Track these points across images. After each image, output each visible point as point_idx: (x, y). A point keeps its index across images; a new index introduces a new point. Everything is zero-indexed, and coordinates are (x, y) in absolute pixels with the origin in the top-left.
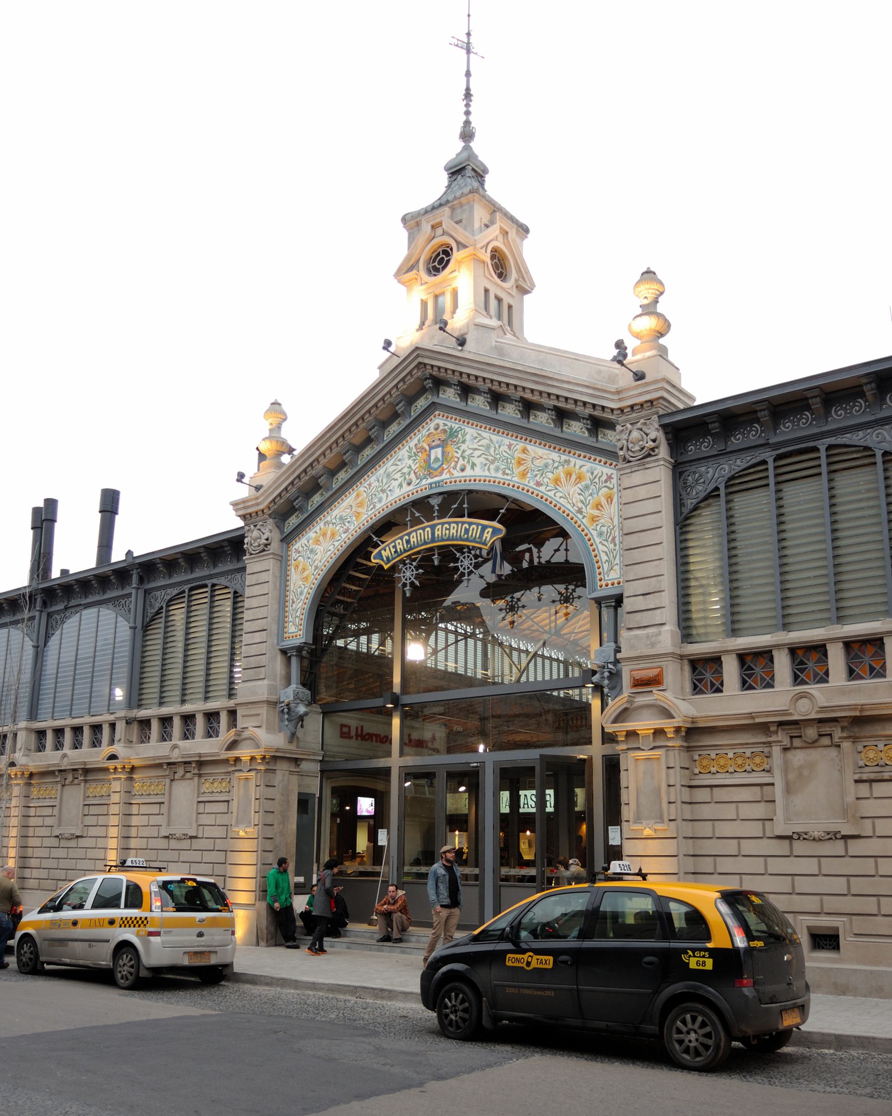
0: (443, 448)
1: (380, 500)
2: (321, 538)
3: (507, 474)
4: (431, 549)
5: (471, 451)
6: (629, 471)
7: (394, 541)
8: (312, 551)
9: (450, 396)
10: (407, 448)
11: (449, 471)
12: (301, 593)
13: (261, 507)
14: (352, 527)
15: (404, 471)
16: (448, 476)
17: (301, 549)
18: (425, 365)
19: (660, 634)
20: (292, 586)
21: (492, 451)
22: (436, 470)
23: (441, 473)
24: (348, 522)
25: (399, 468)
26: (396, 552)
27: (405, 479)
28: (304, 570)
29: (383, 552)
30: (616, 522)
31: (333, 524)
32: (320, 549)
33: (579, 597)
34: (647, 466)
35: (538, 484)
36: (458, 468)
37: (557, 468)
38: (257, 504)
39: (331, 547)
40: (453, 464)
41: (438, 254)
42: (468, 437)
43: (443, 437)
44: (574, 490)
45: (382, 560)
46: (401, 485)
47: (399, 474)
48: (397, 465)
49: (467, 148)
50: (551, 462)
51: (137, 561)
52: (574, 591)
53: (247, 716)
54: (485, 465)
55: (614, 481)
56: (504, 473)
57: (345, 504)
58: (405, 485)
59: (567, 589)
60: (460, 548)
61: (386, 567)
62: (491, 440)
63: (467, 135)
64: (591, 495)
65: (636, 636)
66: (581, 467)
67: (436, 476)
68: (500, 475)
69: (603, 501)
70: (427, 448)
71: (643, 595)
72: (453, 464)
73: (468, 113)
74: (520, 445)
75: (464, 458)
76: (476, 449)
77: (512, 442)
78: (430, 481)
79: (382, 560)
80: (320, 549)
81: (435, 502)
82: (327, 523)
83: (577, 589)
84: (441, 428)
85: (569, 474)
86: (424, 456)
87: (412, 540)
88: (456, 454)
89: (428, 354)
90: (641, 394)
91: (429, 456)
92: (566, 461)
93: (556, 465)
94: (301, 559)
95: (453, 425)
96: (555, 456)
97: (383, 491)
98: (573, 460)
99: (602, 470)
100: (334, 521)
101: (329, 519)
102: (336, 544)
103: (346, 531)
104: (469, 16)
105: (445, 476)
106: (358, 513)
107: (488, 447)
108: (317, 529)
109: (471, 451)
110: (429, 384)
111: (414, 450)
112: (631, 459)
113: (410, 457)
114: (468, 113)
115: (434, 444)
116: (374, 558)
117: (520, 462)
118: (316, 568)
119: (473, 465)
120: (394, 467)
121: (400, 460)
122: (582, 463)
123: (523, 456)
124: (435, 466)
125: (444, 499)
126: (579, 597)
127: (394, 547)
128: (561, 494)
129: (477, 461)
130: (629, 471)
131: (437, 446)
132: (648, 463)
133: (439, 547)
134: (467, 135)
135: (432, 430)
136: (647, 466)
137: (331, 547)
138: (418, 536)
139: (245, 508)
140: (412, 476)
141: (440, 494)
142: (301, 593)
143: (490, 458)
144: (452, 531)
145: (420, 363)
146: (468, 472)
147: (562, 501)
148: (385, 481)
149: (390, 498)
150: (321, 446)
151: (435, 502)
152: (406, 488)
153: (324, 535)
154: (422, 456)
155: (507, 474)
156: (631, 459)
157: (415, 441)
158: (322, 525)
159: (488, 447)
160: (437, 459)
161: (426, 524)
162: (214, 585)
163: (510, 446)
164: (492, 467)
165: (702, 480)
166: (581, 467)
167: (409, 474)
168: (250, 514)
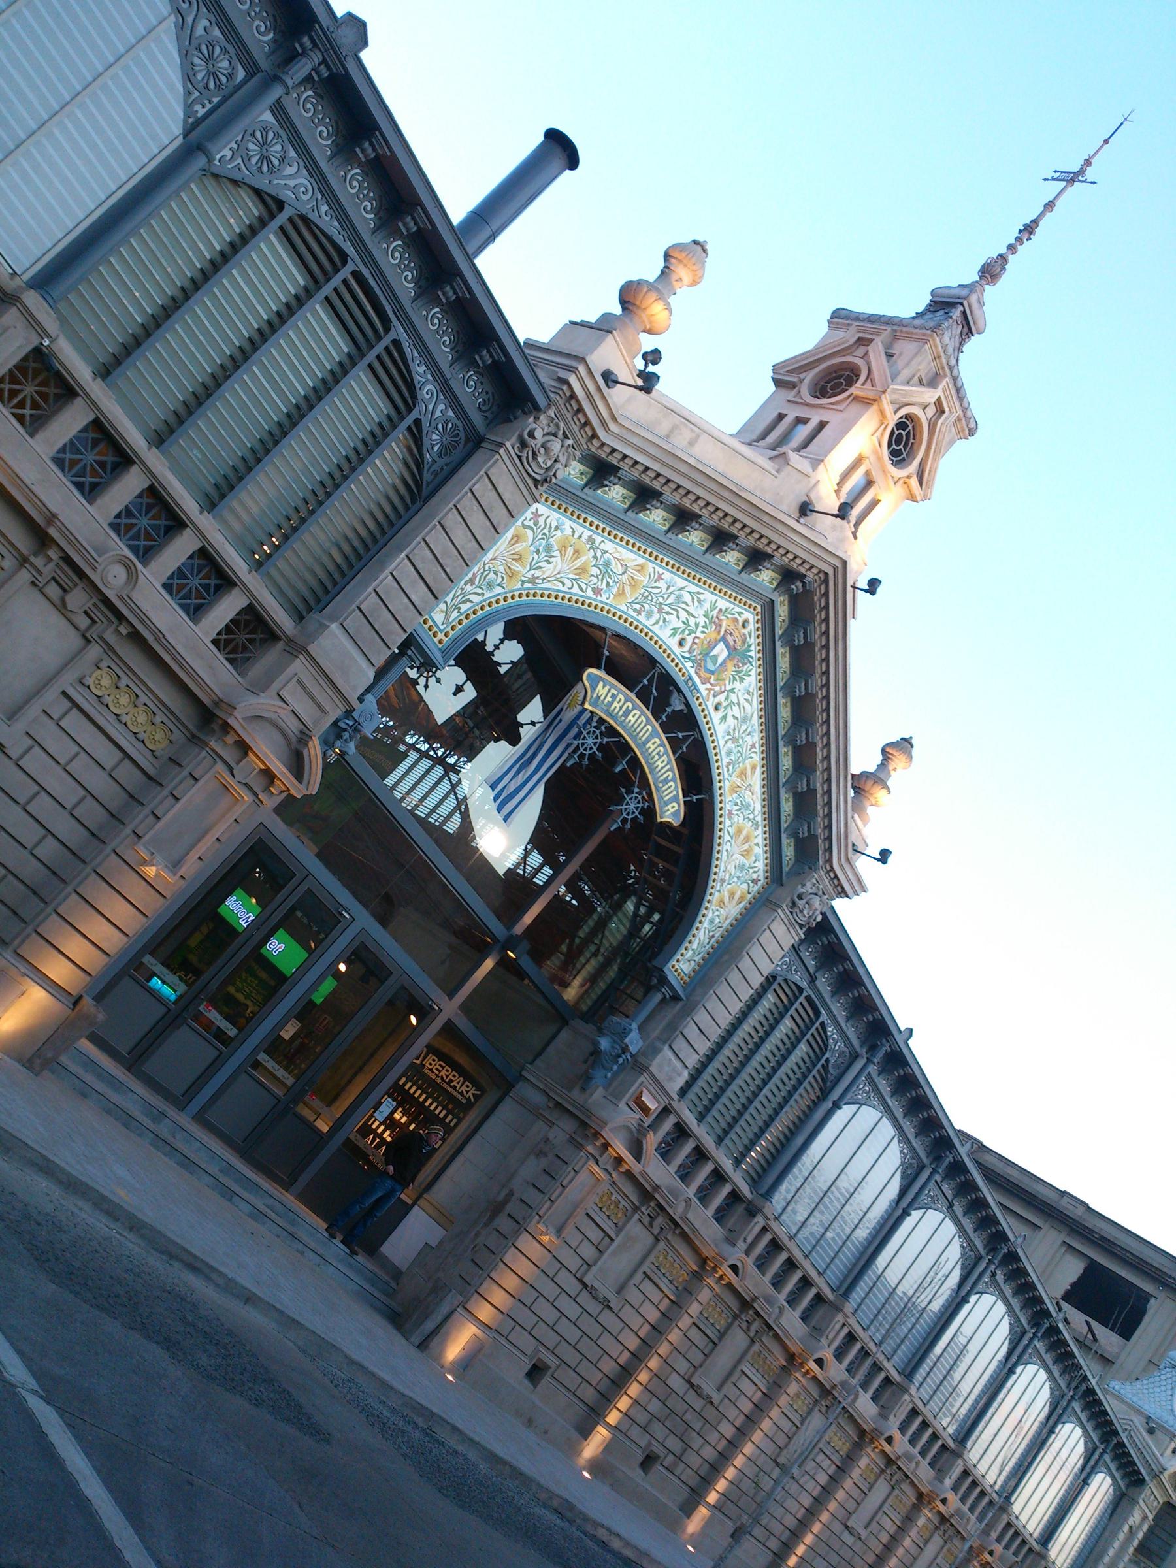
1: (649, 615)
2: (570, 550)
8: (548, 548)
13: (601, 433)
14: (603, 598)
16: (704, 693)
17: (541, 520)
21: (744, 727)
25: (691, 609)
29: (601, 684)
30: (725, 926)
31: (595, 557)
32: (557, 565)
35: (730, 813)
36: (717, 700)
38: (604, 424)
39: (568, 583)
40: (717, 688)
44: (738, 859)
45: (594, 689)
46: (675, 630)
47: (683, 615)
51: (351, 66)
53: (304, 687)
54: (729, 734)
55: (756, 888)
56: (729, 764)
57: (627, 555)
63: (991, 271)
64: (738, 878)
66: (757, 845)
67: (699, 676)
68: (725, 760)
69: (737, 897)
72: (717, 688)
75: (727, 699)
78: (692, 671)
81: (677, 705)
84: (746, 631)
85: (747, 839)
86: (714, 636)
87: (630, 717)
90: (849, 881)
93: (751, 816)
95: (752, 648)
98: (760, 831)
100: (599, 554)
101: (598, 539)
102: (576, 589)
103: (597, 591)
104: (1106, 141)
105: (702, 688)
107: (745, 720)
108: (579, 530)
109: (735, 701)
111: (715, 613)
113: (706, 616)
114: (1012, 248)
117: (743, 774)
118: (532, 580)
119: (724, 718)
123: (749, 772)
127: (614, 697)
129: (730, 719)
131: (727, 646)
132: (794, 928)
134: (991, 271)
139: (589, 396)
140: (689, 639)
141: (687, 705)
144: (659, 763)
146: (716, 717)
147: (725, 853)
149: (655, 629)
150: (710, 491)
152: (673, 643)
160: (716, 657)
163: (753, 746)
164: (730, 744)
166: (757, 845)
168: (580, 410)
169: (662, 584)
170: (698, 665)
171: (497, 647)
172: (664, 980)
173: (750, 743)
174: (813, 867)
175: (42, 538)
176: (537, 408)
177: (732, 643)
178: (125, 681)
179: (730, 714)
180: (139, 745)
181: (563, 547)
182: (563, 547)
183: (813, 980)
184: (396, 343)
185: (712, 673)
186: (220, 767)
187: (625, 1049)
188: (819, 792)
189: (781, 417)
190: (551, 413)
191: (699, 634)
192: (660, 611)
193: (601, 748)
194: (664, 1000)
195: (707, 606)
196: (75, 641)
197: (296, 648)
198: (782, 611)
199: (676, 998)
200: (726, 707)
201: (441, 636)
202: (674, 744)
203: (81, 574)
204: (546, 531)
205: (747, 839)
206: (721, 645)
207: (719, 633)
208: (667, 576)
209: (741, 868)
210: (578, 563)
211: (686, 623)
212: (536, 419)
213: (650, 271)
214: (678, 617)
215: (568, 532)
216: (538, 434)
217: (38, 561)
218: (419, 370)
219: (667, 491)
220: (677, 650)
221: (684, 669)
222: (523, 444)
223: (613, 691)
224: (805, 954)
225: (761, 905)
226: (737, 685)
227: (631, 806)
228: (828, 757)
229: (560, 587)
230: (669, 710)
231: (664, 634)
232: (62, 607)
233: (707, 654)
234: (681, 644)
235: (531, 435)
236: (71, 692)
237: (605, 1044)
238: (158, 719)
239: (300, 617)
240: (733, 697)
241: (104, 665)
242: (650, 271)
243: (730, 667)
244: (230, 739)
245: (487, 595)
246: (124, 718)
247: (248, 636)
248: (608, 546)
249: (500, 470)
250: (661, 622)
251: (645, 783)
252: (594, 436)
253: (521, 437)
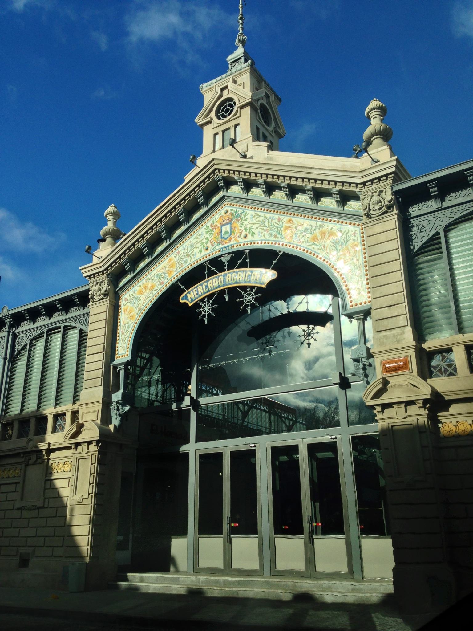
0: (231, 224)
1: (186, 262)
3: (278, 238)
4: (222, 292)
5: (251, 225)
6: (371, 224)
7: (196, 287)
8: (137, 298)
9: (236, 190)
10: (205, 227)
11: (236, 240)
12: (129, 327)
14: (166, 281)
15: (203, 241)
16: (235, 242)
17: (129, 298)
18: (219, 169)
19: (404, 333)
20: (122, 322)
21: (266, 224)
22: (226, 239)
23: (230, 240)
24: (163, 278)
25: (199, 240)
26: (197, 294)
27: (204, 246)
28: (131, 311)
29: (188, 295)
32: (142, 297)
33: (317, 333)
34: (385, 220)
37: (314, 230)
39: (151, 295)
40: (238, 234)
41: (226, 107)
42: (248, 217)
43: (231, 218)
45: (188, 300)
46: (201, 251)
47: (199, 244)
48: (198, 238)
50: (309, 227)
52: (313, 328)
56: (275, 237)
57: (161, 266)
58: (203, 250)
59: (308, 327)
60: (244, 288)
61: (190, 305)
62: (265, 217)
65: (385, 336)
67: (226, 243)
68: (272, 238)
70: (220, 226)
71: (388, 307)
74: (287, 218)
76: (254, 224)
77: (281, 217)
78: (221, 246)
79: (188, 300)
80: (142, 297)
81: (225, 259)
82: (148, 279)
83: (316, 328)
87: (209, 285)
88: (240, 228)
89: (221, 162)
91: (221, 231)
92: (320, 226)
94: (129, 304)
96: (312, 222)
97: (188, 256)
100: (153, 278)
101: (149, 277)
102: (154, 292)
105: (232, 243)
106: (170, 271)
108: (141, 284)
109: (250, 225)
110: (221, 183)
112: (372, 216)
113: (207, 233)
115: (224, 223)
116: (182, 300)
118: (140, 309)
120: (196, 240)
121: (200, 235)
122: (333, 226)
124: (226, 236)
125: (232, 257)
126: (317, 333)
128: (318, 247)
130: (371, 224)
131: (227, 224)
133: (228, 288)
135: (223, 214)
136: (385, 220)
137: (151, 295)
138: (214, 283)
139: (90, 270)
140: (209, 244)
141: (229, 253)
142: (129, 327)
143: (265, 228)
145: (216, 169)
146: (249, 238)
147: (319, 251)
148: (189, 249)
151: (225, 259)
152: (204, 252)
153: (145, 287)
154: (216, 231)
155: (278, 238)
156: (372, 216)
157: (211, 222)
158: (144, 281)
159: (263, 221)
160: (226, 232)
161: (219, 274)
162: (65, 327)
165: (424, 229)
167: (207, 243)
168: (94, 274)
171: (288, 308)
173: (276, 221)
177: (227, 221)
179: (253, 230)
185: (231, 235)
188: (314, 185)
191: (210, 239)
195: (205, 231)
200: (249, 232)
202: (243, 265)
204: (132, 297)
207: (218, 227)
214: (196, 248)
223: (194, 290)
226: (246, 223)
229: (149, 299)
230: (227, 263)
231: (198, 256)
233: (222, 237)
245: (130, 330)
248: (153, 273)
250: (192, 257)
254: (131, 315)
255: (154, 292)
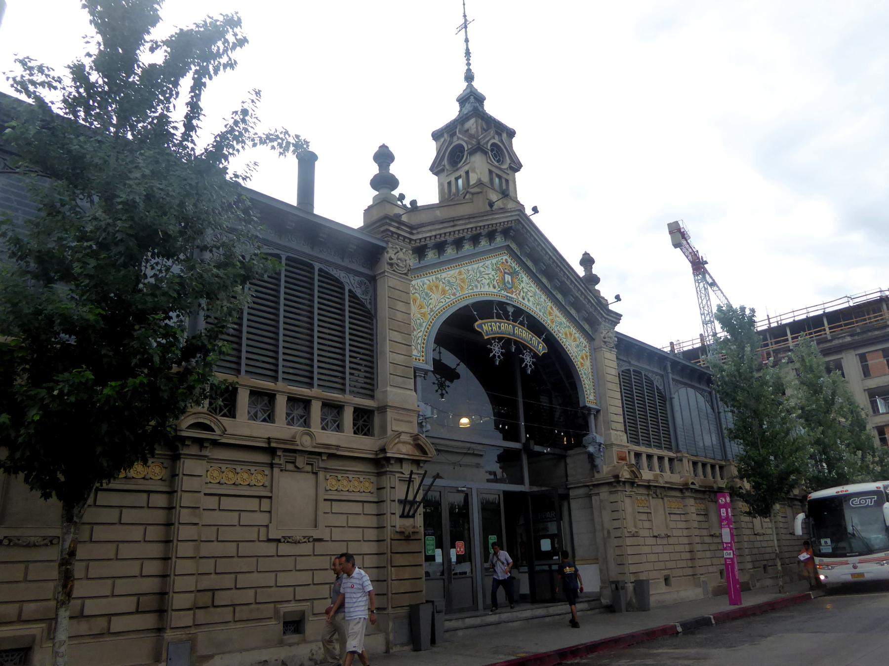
8: (427, 294)
45: (482, 329)
47: (486, 277)
49: (470, 86)
53: (398, 420)
57: (452, 272)
63: (469, 77)
73: (468, 64)
81: (511, 310)
85: (571, 334)
99: (584, 342)
102: (447, 300)
103: (454, 294)
105: (513, 296)
108: (430, 278)
114: (468, 64)
118: (432, 310)
119: (529, 300)
124: (509, 286)
129: (531, 299)
134: (469, 77)
141: (514, 306)
146: (526, 302)
149: (482, 290)
152: (491, 289)
168: (399, 235)
169: (471, 272)
170: (505, 290)
172: (589, 409)
174: (599, 324)
175: (270, 451)
176: (384, 249)
178: (339, 476)
180: (364, 494)
181: (431, 289)
182: (431, 289)
183: (629, 363)
184: (320, 270)
186: (397, 475)
187: (600, 444)
189: (449, 183)
190: (390, 245)
192: (478, 282)
193: (502, 348)
194: (595, 416)
196: (312, 477)
197: (383, 409)
198: (513, 246)
199: (598, 411)
201: (421, 358)
202: (522, 323)
203: (295, 451)
205: (571, 334)
206: (506, 276)
208: (470, 268)
209: (578, 346)
210: (440, 290)
211: (490, 278)
212: (387, 252)
213: (375, 169)
215: (428, 282)
216: (393, 256)
217: (276, 461)
218: (335, 272)
219: (447, 238)
220: (495, 291)
221: (501, 296)
222: (391, 265)
224: (622, 358)
225: (595, 351)
227: (528, 359)
228: (572, 281)
232: (298, 469)
234: (494, 287)
235: (391, 259)
236: (326, 497)
237: (591, 449)
238: (361, 479)
239: (372, 397)
240: (525, 290)
241: (328, 477)
242: (375, 169)
243: (515, 280)
244: (392, 462)
246: (351, 490)
247: (364, 421)
248: (444, 275)
249: (389, 283)
251: (525, 347)
252: (411, 240)
253: (388, 263)
254: (423, 310)
255: (447, 300)
